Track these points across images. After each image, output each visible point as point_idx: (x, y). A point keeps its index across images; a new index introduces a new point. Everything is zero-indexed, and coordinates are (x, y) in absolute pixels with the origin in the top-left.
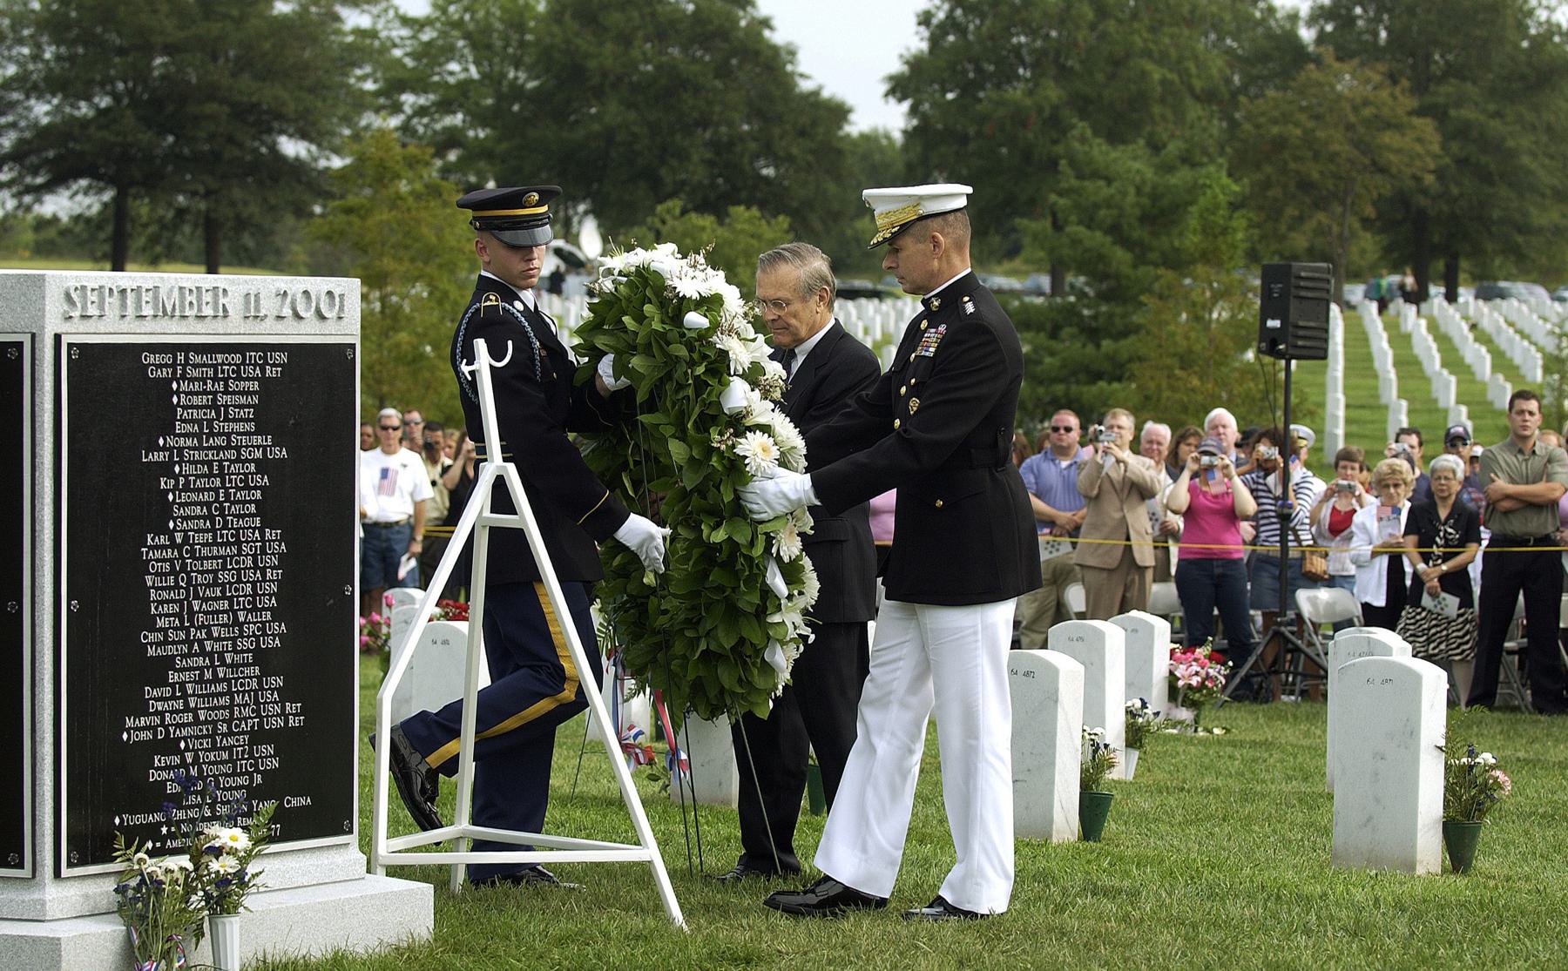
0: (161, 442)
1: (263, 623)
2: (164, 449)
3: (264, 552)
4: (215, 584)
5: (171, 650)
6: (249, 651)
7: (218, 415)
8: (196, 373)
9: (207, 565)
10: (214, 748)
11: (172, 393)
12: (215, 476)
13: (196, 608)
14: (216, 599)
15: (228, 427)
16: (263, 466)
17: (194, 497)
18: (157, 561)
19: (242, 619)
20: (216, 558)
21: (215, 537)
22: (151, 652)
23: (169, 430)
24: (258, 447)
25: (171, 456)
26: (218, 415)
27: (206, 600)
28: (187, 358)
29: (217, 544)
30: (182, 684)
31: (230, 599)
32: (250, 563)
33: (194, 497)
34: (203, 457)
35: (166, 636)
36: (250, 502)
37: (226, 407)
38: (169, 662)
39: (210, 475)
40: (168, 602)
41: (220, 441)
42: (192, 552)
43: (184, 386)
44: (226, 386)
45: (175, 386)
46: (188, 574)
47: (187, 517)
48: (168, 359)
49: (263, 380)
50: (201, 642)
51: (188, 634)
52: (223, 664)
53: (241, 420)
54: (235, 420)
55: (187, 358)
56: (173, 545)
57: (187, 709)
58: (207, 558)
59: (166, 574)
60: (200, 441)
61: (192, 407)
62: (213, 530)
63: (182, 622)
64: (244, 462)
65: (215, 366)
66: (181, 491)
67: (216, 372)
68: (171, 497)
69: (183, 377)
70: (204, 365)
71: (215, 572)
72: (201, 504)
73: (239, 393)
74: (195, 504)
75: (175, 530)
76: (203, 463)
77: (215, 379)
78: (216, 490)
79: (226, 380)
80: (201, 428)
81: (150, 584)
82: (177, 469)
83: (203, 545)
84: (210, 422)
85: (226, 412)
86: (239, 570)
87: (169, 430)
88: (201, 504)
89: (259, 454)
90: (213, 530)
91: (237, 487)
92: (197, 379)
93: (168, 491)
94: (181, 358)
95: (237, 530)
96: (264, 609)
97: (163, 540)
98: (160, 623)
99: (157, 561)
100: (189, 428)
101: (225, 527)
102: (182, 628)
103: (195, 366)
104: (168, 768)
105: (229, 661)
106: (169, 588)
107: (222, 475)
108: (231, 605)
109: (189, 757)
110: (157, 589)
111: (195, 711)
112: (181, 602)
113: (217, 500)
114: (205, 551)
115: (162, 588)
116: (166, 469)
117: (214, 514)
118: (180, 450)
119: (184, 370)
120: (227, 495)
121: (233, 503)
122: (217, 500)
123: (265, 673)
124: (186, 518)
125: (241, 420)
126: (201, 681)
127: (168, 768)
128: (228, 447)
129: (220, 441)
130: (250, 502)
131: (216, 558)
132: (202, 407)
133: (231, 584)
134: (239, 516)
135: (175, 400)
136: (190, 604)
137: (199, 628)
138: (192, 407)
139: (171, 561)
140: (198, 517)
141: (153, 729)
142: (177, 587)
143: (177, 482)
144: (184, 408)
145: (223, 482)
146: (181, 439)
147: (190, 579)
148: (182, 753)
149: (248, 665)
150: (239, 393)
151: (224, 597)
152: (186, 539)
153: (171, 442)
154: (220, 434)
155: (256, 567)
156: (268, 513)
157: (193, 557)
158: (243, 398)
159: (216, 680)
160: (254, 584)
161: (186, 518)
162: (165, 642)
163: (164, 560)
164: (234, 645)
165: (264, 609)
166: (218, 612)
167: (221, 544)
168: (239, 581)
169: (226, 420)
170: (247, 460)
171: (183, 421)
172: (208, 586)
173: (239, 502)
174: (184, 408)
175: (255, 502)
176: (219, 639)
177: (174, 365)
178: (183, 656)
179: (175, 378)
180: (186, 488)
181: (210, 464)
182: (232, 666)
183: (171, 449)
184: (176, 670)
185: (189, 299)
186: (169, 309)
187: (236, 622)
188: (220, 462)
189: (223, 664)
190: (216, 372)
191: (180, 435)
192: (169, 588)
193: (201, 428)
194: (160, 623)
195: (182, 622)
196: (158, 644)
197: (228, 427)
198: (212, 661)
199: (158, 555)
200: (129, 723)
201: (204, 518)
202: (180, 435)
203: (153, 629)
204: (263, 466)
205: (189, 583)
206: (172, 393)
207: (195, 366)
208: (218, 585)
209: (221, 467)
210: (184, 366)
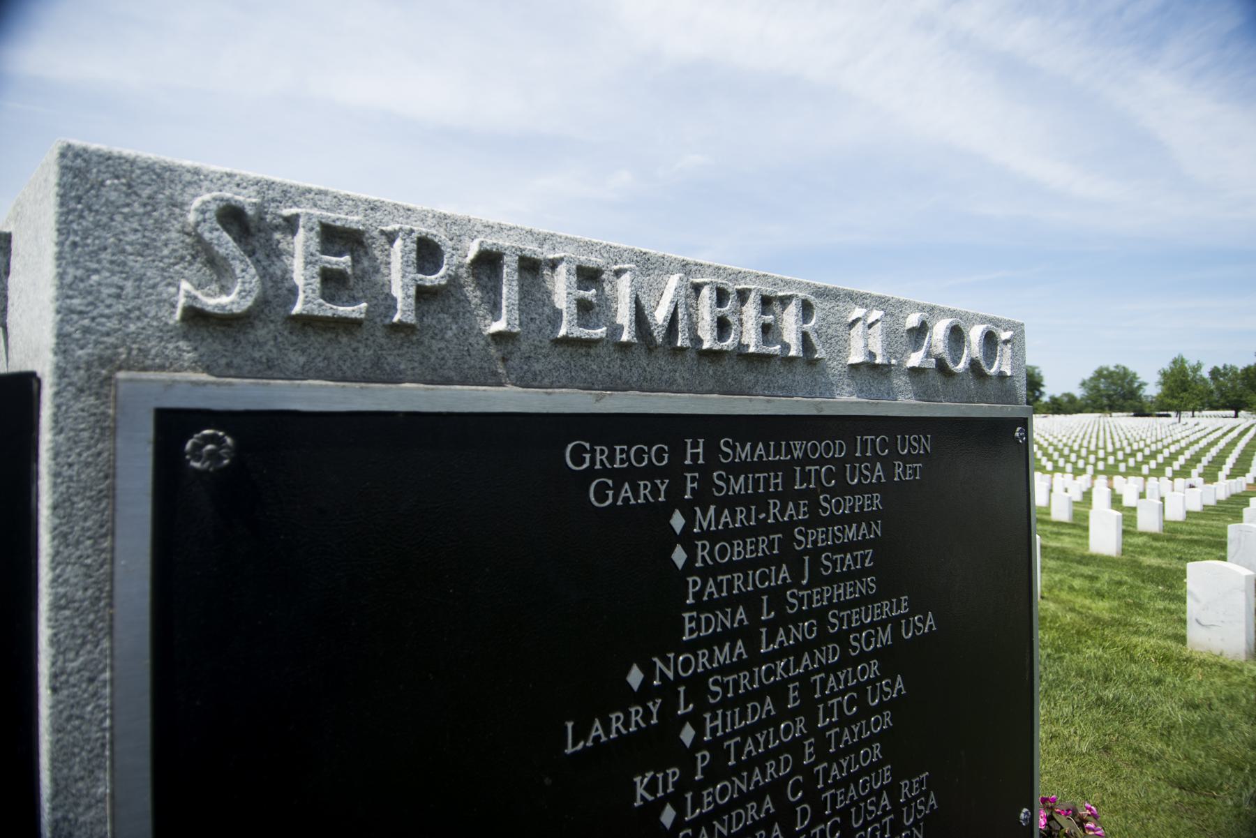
0: (635, 677)
7: (797, 574)
8: (738, 485)
11: (671, 539)
15: (820, 597)
24: (883, 624)
26: (797, 574)
28: (712, 450)
37: (815, 553)
43: (707, 519)
44: (814, 506)
45: (678, 522)
53: (850, 575)
54: (834, 579)
55: (712, 450)
60: (752, 645)
61: (731, 567)
64: (855, 662)
65: (787, 469)
68: (668, 816)
69: (703, 498)
74: (742, 801)
77: (786, 496)
80: (753, 612)
82: (687, 735)
84: (777, 596)
85: (816, 564)
94: (695, 450)
100: (722, 620)
103: (736, 469)
116: (657, 746)
118: (697, 687)
119: (705, 481)
121: (835, 758)
125: (850, 575)
128: (823, 638)
132: (754, 564)
135: (679, 556)
138: (731, 567)
144: (708, 572)
146: (705, 647)
170: (864, 657)
171: (699, 606)
179: (675, 500)
181: (778, 691)
183: (668, 689)
188: (804, 678)
190: (789, 480)
191: (693, 647)
193: (753, 612)
197: (820, 597)
202: (693, 647)
204: (890, 659)
206: (671, 539)
207: (736, 469)
209: (806, 686)
210: (705, 473)
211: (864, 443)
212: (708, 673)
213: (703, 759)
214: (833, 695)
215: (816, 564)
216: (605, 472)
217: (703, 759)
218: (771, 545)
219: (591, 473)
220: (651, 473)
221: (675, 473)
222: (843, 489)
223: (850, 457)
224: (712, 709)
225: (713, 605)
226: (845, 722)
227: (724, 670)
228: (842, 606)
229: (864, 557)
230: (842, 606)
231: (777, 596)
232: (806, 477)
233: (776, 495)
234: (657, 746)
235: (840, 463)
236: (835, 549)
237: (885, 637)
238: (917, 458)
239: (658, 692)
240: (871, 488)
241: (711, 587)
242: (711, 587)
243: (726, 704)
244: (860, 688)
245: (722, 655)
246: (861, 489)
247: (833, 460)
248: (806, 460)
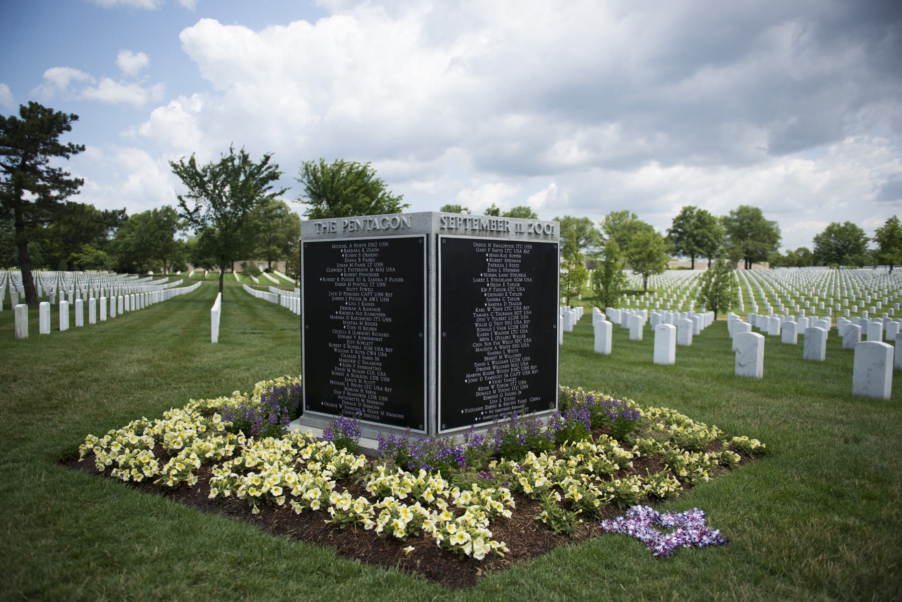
4: (504, 325)
5: (486, 349)
9: (501, 319)
10: (503, 383)
15: (509, 270)
22: (477, 350)
23: (486, 271)
27: (500, 331)
30: (490, 362)
38: (485, 354)
39: (502, 287)
41: (505, 275)
49: (522, 254)
50: (498, 346)
52: (507, 353)
56: (486, 312)
57: (492, 369)
62: (503, 307)
77: (504, 253)
79: (508, 254)
84: (502, 269)
87: (486, 271)
89: (521, 280)
90: (503, 307)
97: (482, 310)
98: (481, 340)
104: (484, 391)
109: (493, 387)
111: (495, 371)
117: (503, 301)
118: (490, 278)
123: (523, 356)
126: (498, 359)
127: (484, 391)
128: (509, 277)
129: (505, 275)
141: (478, 378)
142: (488, 327)
146: (490, 273)
148: (490, 386)
152: (492, 310)
153: (485, 275)
158: (515, 260)
159: (504, 359)
162: (483, 346)
177: (487, 248)
180: (492, 291)
181: (502, 283)
189: (507, 353)
194: (481, 340)
197: (509, 270)
200: (468, 376)
231: (502, 269)
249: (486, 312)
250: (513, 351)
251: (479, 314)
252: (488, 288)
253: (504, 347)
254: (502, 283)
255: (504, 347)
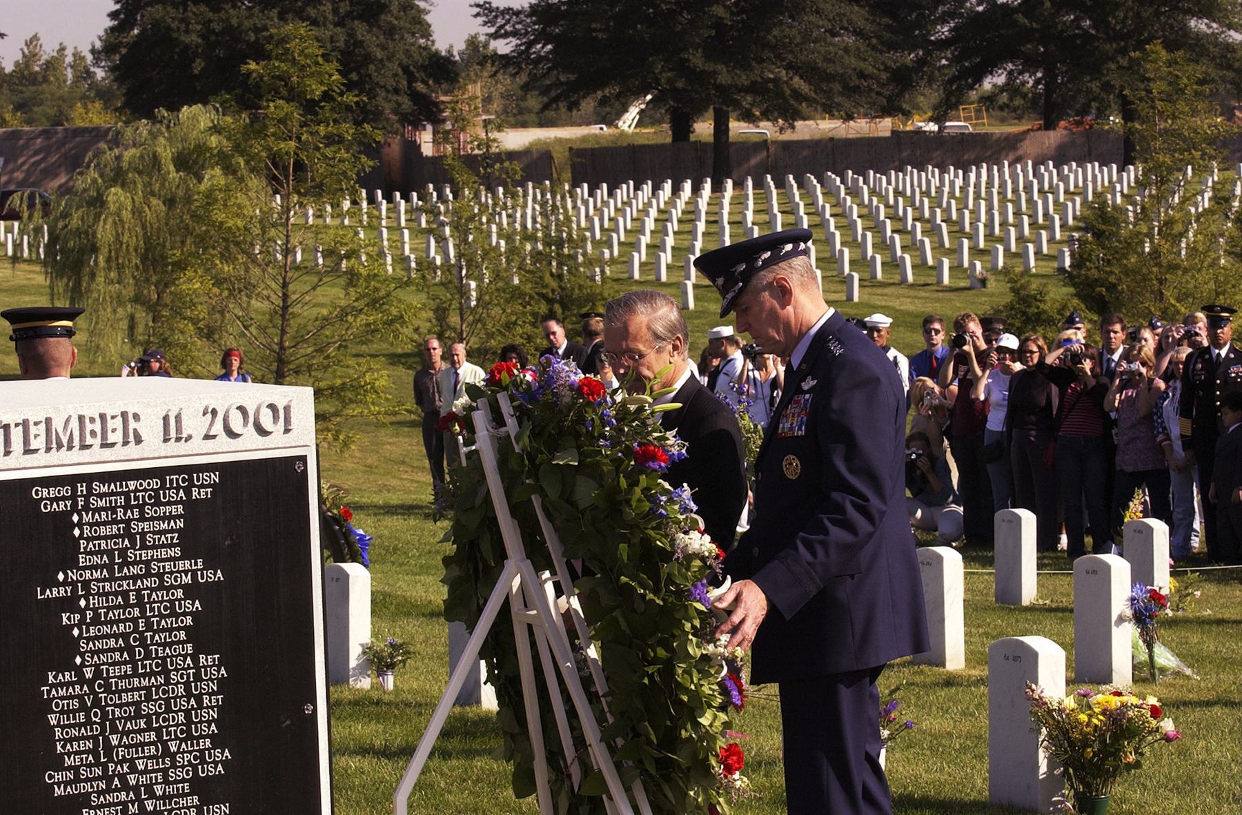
0: (61, 577)
1: (202, 751)
2: (65, 583)
3: (198, 677)
4: (138, 715)
5: (84, 788)
6: (183, 781)
8: (101, 503)
11: (73, 526)
12: (132, 606)
13: (115, 742)
14: (140, 731)
16: (191, 591)
17: (106, 629)
18: (62, 698)
19: (174, 749)
20: (138, 689)
21: (135, 669)
22: (58, 791)
24: (186, 572)
25: (75, 590)
27: (127, 733)
28: (89, 489)
29: (139, 676)
31: (158, 731)
32: (181, 690)
33: (106, 629)
34: (115, 587)
35: (77, 774)
36: (179, 629)
37: (143, 534)
39: (127, 605)
40: (78, 739)
41: (134, 570)
42: (107, 688)
44: (142, 513)
45: (75, 518)
46: (103, 709)
47: (97, 649)
48: (66, 491)
50: (123, 778)
51: (105, 769)
52: (152, 795)
53: (163, 546)
54: (154, 547)
55: (89, 489)
56: (82, 680)
58: (126, 691)
59: (74, 711)
60: (111, 572)
61: (99, 538)
62: (133, 662)
63: (96, 757)
64: (168, 589)
65: (127, 495)
66: (88, 625)
67: (128, 500)
68: (76, 632)
69: (86, 508)
70: (113, 494)
71: (137, 704)
72: (116, 636)
73: (159, 518)
74: (108, 636)
75: (83, 664)
76: (116, 594)
77: (127, 507)
78: (135, 621)
79: (141, 507)
80: (111, 558)
81: (53, 722)
82: (83, 603)
83: (120, 677)
84: (123, 552)
85: (143, 540)
86: (169, 699)
88: (116, 636)
90: (133, 662)
91: (161, 616)
92: (103, 509)
93: (71, 627)
95: (164, 659)
96: (201, 737)
98: (68, 762)
99: (62, 698)
100: (96, 560)
101: (148, 656)
102: (97, 763)
105: (159, 793)
106: (80, 725)
107: (140, 604)
108: (159, 736)
110: (63, 727)
112: (95, 738)
113: (136, 630)
114: (122, 684)
115: (70, 726)
116: (69, 604)
117: (133, 647)
118: (86, 584)
119: (87, 502)
120: (149, 626)
121: (155, 632)
122: (136, 630)
124: (99, 652)
125: (163, 546)
128: (148, 575)
129: (134, 570)
130: (179, 629)
131: (138, 689)
132: (112, 537)
133: (158, 715)
134: (164, 645)
135: (77, 532)
136: (107, 741)
137: (121, 762)
138: (99, 538)
139: (80, 698)
140: (113, 650)
142: (89, 722)
143: (84, 616)
144: (88, 539)
145: (143, 611)
147: (105, 715)
149: (184, 795)
150: (159, 518)
151: (149, 728)
152: (98, 674)
154: (135, 563)
155: (189, 694)
156: (200, 638)
157: (108, 689)
160: (187, 713)
161: (99, 652)
162: (77, 780)
163: (71, 697)
164: (166, 776)
165: (201, 737)
166: (143, 744)
167: (144, 675)
168: (168, 710)
169: (144, 547)
170: (172, 587)
172: (129, 718)
173: (164, 630)
174: (88, 539)
175: (185, 628)
176: (146, 772)
178: (100, 793)
180: (96, 621)
181: (125, 594)
182: (164, 797)
183: (73, 584)
184: (91, 808)
185: (89, 427)
186: (65, 440)
187: (166, 752)
188: (139, 591)
189: (152, 795)
190: (128, 500)
191: (84, 568)
192: (80, 725)
193: (111, 558)
194: (68, 762)
195: (96, 757)
196: (68, 783)
198: (138, 795)
199: (62, 692)
201: (121, 650)
202: (84, 568)
203: (60, 767)
204: (191, 591)
205: (105, 715)
206: (73, 526)
208: (142, 717)
209: (139, 596)
210: (87, 497)
211: (171, 481)
212: (90, 581)
213: (89, 614)
214: (154, 602)
215: (143, 540)
216: (46, 499)
217: (89, 614)
218: (119, 529)
219: (42, 499)
220: (64, 498)
221: (74, 497)
222: (158, 503)
223: (163, 487)
224: (93, 595)
225: (91, 553)
226: (161, 616)
227: (98, 580)
228: (159, 561)
229: (172, 538)
230: (159, 561)
231: (123, 552)
232: (137, 498)
233: (121, 507)
234: (69, 604)
235: (156, 491)
236: (154, 533)
237: (187, 579)
238: (209, 486)
239: (69, 584)
240: (176, 503)
241: (91, 545)
242: (91, 545)
243: (98, 594)
244: (172, 602)
245: (97, 575)
246: (169, 503)
247: (152, 490)
248: (136, 490)
249: (82, 680)
250: (170, 790)
251: (58, 688)
252: (82, 612)
253: (143, 780)
254: (125, 594)
255: (143, 780)
